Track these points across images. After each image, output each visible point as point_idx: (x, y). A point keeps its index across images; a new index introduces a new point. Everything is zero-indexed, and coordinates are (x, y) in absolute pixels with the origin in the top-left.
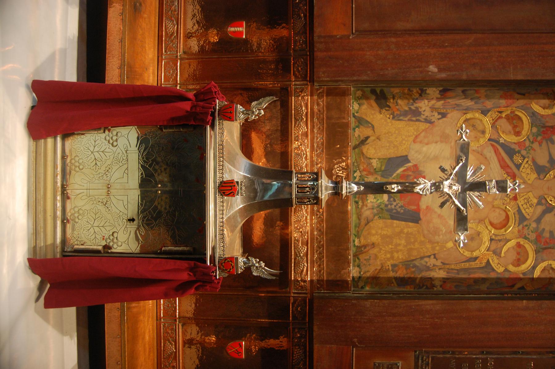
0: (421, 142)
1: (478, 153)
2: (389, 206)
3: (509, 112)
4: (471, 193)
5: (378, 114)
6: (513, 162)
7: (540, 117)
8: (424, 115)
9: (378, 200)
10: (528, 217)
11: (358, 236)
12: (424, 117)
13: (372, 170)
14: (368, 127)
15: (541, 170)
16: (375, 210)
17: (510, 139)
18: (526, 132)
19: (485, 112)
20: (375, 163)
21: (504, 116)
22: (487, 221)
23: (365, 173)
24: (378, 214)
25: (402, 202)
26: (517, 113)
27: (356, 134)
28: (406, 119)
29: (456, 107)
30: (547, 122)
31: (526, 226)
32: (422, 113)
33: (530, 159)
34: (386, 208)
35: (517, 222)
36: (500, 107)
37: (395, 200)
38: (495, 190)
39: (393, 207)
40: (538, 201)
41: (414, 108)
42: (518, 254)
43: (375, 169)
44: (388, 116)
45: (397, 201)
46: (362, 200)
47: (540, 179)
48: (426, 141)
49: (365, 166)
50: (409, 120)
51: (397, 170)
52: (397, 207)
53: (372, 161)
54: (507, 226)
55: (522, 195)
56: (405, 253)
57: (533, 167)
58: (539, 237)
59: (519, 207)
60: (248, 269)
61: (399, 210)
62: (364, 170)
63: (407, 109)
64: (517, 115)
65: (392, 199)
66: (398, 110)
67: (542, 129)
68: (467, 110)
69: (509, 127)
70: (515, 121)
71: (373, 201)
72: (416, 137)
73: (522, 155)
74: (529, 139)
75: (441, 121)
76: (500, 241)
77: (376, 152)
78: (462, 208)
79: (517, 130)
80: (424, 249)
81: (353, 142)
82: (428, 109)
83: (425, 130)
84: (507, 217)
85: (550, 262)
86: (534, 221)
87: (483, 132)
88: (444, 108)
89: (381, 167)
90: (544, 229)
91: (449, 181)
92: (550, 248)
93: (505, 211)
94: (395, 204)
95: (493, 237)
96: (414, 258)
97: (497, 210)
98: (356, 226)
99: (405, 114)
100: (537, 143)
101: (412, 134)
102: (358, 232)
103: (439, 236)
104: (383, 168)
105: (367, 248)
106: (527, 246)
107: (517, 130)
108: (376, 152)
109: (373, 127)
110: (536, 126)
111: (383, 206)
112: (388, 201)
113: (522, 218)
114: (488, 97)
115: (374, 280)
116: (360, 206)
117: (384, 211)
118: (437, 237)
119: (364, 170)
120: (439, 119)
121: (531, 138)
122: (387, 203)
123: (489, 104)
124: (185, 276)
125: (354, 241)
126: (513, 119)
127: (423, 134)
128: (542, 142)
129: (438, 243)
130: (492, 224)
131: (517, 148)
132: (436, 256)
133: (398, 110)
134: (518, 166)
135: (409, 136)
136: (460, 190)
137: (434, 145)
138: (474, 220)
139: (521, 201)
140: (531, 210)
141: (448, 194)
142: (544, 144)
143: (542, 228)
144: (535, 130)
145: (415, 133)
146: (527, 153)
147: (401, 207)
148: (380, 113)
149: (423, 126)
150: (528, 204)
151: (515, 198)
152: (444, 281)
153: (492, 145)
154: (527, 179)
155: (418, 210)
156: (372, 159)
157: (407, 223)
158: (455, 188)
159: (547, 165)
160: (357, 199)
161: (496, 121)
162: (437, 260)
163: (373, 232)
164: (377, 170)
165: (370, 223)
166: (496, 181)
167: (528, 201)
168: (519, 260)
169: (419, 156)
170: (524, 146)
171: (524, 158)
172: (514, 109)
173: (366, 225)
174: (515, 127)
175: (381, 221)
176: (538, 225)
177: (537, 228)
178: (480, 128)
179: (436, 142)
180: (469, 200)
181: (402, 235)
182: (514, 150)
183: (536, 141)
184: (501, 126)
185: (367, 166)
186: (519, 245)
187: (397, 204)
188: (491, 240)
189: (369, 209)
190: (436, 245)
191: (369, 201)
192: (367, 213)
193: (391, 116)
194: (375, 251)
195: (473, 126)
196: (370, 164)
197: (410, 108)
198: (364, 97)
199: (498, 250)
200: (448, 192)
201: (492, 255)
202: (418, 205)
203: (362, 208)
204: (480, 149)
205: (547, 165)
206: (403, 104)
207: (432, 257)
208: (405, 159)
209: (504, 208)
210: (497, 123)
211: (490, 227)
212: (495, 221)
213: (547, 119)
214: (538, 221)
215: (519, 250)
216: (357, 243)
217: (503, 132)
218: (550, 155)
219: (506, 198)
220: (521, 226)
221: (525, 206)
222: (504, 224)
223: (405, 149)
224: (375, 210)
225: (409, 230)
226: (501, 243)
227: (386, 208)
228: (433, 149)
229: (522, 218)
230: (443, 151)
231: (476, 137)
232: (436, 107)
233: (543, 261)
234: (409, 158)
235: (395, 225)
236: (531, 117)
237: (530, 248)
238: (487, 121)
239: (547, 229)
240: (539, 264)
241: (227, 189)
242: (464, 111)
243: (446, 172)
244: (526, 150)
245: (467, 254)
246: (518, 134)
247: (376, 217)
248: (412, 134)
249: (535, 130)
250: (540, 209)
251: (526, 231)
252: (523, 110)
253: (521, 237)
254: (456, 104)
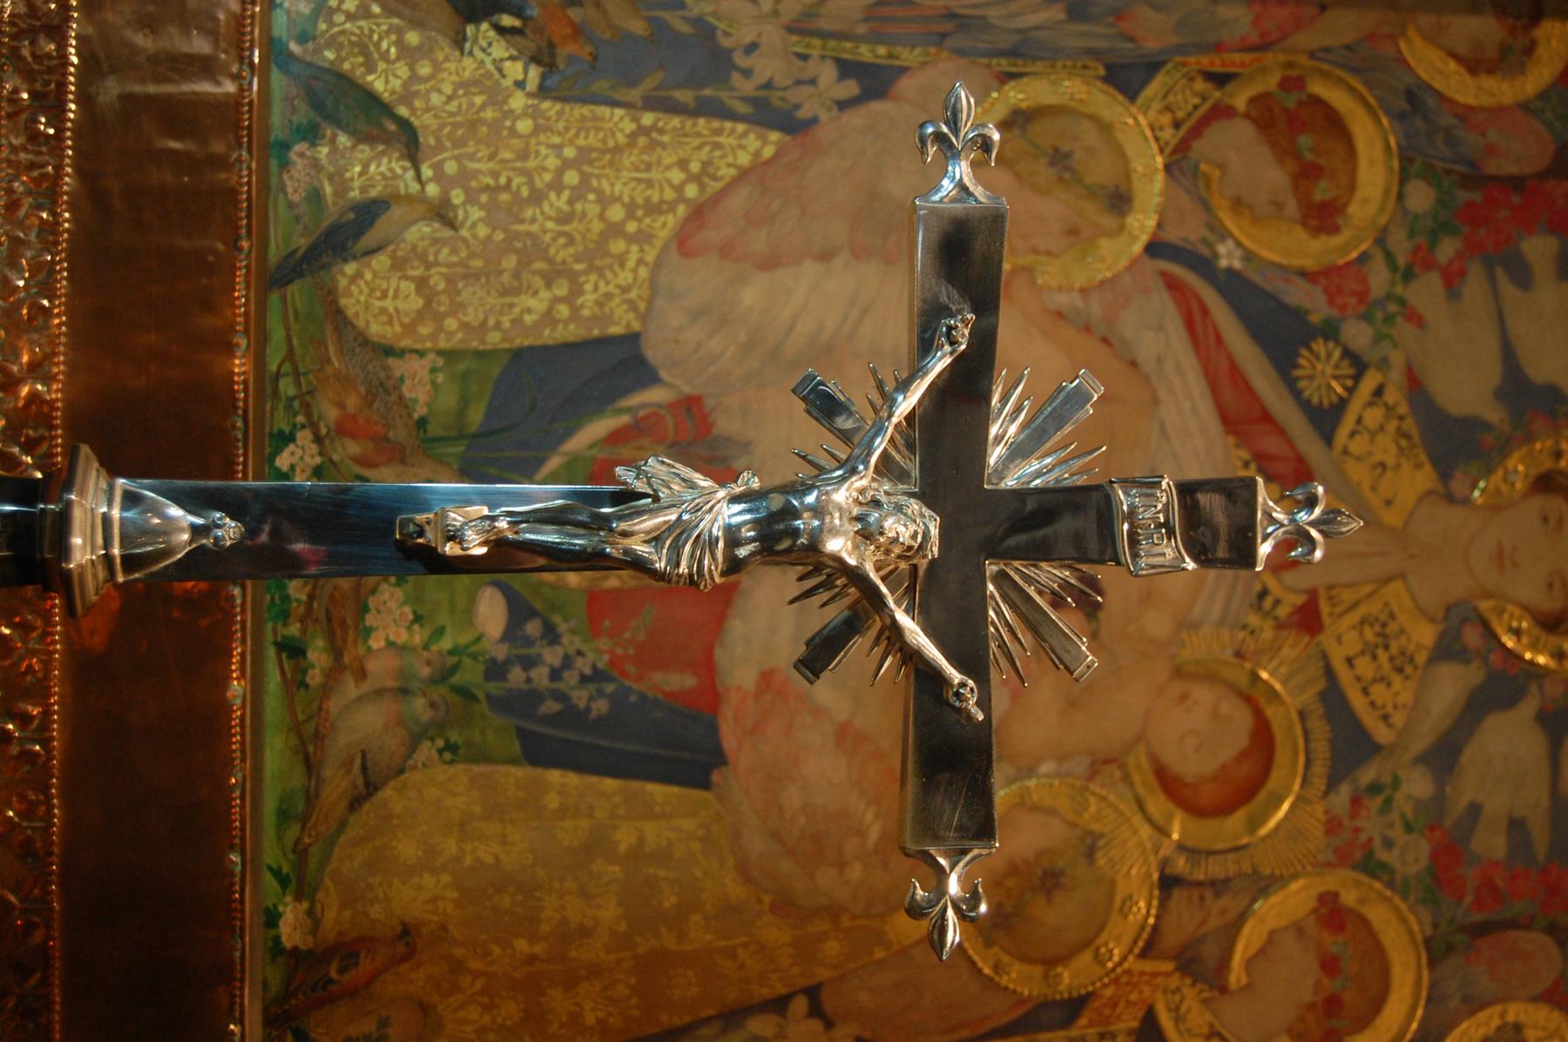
0: (726, 251)
1: (1087, 329)
2: (516, 676)
3: (1271, 82)
4: (1017, 569)
5: (444, 49)
6: (1296, 394)
7: (1447, 120)
8: (747, 73)
9: (439, 632)
10: (1382, 734)
11: (300, 882)
12: (747, 87)
13: (399, 434)
14: (387, 139)
15: (1452, 445)
16: (419, 704)
17: (1273, 246)
18: (1372, 208)
19: (1126, 77)
20: (420, 385)
21: (1240, 102)
22: (1139, 762)
23: (354, 448)
24: (435, 728)
25: (604, 643)
26: (1318, 88)
28: (635, 95)
30: (1491, 150)
31: (1375, 788)
32: (739, 59)
33: (1396, 375)
34: (494, 688)
35: (1319, 769)
36: (1219, 47)
37: (551, 635)
38: (1168, 551)
39: (540, 676)
40: (1442, 636)
41: (685, 28)
42: (1330, 965)
43: (422, 422)
44: (515, 70)
45: (571, 642)
46: (330, 635)
47: (1450, 498)
48: (759, 242)
49: (352, 402)
50: (650, 104)
51: (569, 433)
52: (571, 678)
53: (398, 367)
54: (1262, 796)
55: (1348, 596)
56: (621, 990)
57: (1410, 425)
59: (1329, 672)
61: (580, 697)
62: (344, 429)
63: (637, 26)
64: (1318, 101)
65: (533, 628)
66: (578, 31)
67: (1463, 196)
69: (1268, 175)
70: (1305, 141)
71: (402, 637)
72: (698, 213)
73: (1347, 353)
74: (1389, 256)
75: (855, 118)
76: (1218, 886)
78: (956, 676)
79: (1322, 191)
80: (743, 955)
82: (772, 34)
83: (754, 173)
84: (1263, 736)
85: (1516, 1011)
86: (1421, 759)
87: (1119, 201)
88: (875, 38)
89: (461, 412)
90: (1475, 810)
91: (858, 483)
92: (1513, 924)
93: (1253, 698)
94: (552, 656)
95: (1181, 865)
96: (677, 1021)
97: (1204, 695)
98: (284, 815)
100: (1434, 278)
101: (669, 195)
102: (301, 853)
103: (842, 866)
104: (476, 416)
105: (365, 965)
106: (1379, 916)
107: (1322, 191)
109: (409, 143)
110: (1429, 174)
111: (471, 674)
112: (507, 637)
116: (315, 677)
117: (483, 708)
118: (826, 877)
119: (344, 429)
120: (843, 105)
121: (1401, 245)
122: (501, 652)
125: (272, 919)
126: (1295, 123)
127: (739, 201)
128: (1462, 273)
129: (833, 912)
130: (1168, 783)
131: (1314, 303)
132: (826, 996)
133: (578, 31)
134: (1325, 419)
135: (653, 209)
136: (934, 550)
137: (810, 269)
138: (1062, 758)
139: (1342, 637)
140: (1402, 690)
141: (856, 576)
142: (1475, 284)
143: (1464, 801)
144: (1421, 197)
145: (691, 191)
146: (1379, 338)
147: (597, 676)
148: (459, 41)
150: (1383, 656)
151: (1308, 619)
153: (1174, 286)
154: (1375, 501)
155: (710, 695)
156: (401, 353)
157: (635, 785)
158: (898, 528)
159: (1494, 415)
160: (294, 629)
161: (1197, 131)
162: (829, 1024)
163: (407, 850)
164: (434, 429)
165: (387, 793)
166: (1187, 490)
167: (1383, 634)
168: (1332, 1004)
169: (715, 344)
170: (1362, 296)
171: (1359, 366)
172: (1303, 60)
173: (355, 804)
174: (1307, 173)
175: (460, 774)
176: (1440, 785)
177: (1439, 802)
178: (1100, 172)
179: (826, 256)
180: (998, 614)
181: (598, 866)
182: (1298, 314)
183: (1428, 264)
184: (1222, 167)
185: (369, 399)
186: (1332, 913)
187: (567, 662)
188: (1168, 883)
189: (379, 693)
190: (822, 925)
191: (376, 643)
192: (363, 722)
193: (534, 73)
194: (417, 978)
195: (1059, 158)
196: (384, 390)
197: (658, 26)
199: (1211, 952)
200: (852, 562)
201: (1174, 981)
202: (707, 667)
203: (326, 690)
204: (1096, 310)
205: (1494, 415)
207: (800, 1005)
209: (1243, 682)
210: (1200, 146)
211: (1157, 804)
212: (1191, 764)
213: (1493, 136)
214: (1444, 756)
215: (1334, 944)
216: (291, 929)
217: (1238, 205)
218: (1509, 355)
219: (1254, 620)
220: (1345, 791)
221: (1364, 666)
222: (1245, 786)
223: (625, 290)
224: (419, 704)
225: (650, 829)
226: (1224, 901)
227: (494, 688)
229: (1350, 745)
230: (866, 310)
231: (1073, 232)
232: (822, 24)
233: (1474, 1005)
234: (652, 354)
235: (552, 801)
236: (1401, 117)
237: (1396, 929)
238: (1139, 135)
239: (1496, 804)
240: (1452, 1025)
242: (1004, 64)
243: (844, 423)
244: (1367, 317)
245: (1022, 980)
246: (1323, 217)
247: (427, 750)
248: (669, 195)
249: (1421, 197)
250: (1451, 685)
251: (1371, 825)
252: (1355, 71)
253: (1342, 858)
254: (953, 16)
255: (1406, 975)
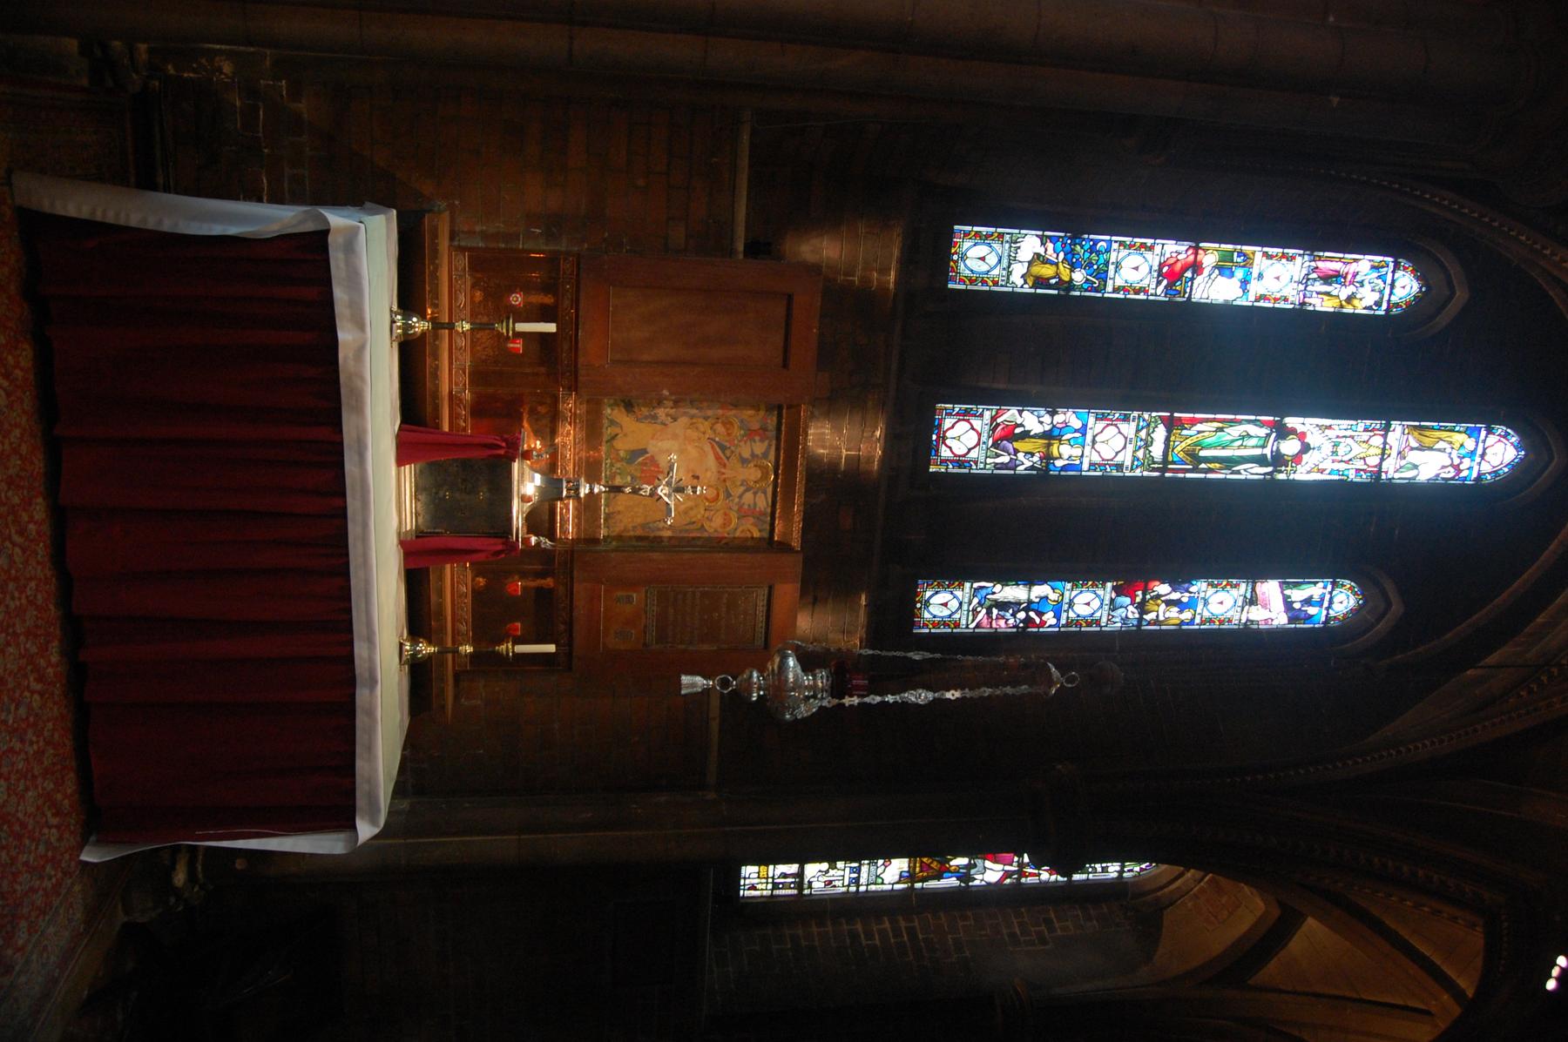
15: (744, 461)
19: (706, 418)
20: (622, 454)
27: (608, 432)
29: (685, 414)
58: (739, 510)
60: (538, 544)
68: (692, 417)
77: (623, 446)
81: (605, 438)
99: (646, 417)
108: (623, 446)
113: (728, 495)
114: (709, 408)
115: (619, 537)
123: (710, 413)
124: (500, 547)
149: (659, 427)
152: (670, 538)
198: (616, 404)
206: (645, 411)
208: (644, 451)
214: (740, 497)
222: (716, 499)
228: (666, 445)
229: (728, 495)
237: (734, 516)
241: (524, 499)
250: (742, 489)
255: (735, 521)
